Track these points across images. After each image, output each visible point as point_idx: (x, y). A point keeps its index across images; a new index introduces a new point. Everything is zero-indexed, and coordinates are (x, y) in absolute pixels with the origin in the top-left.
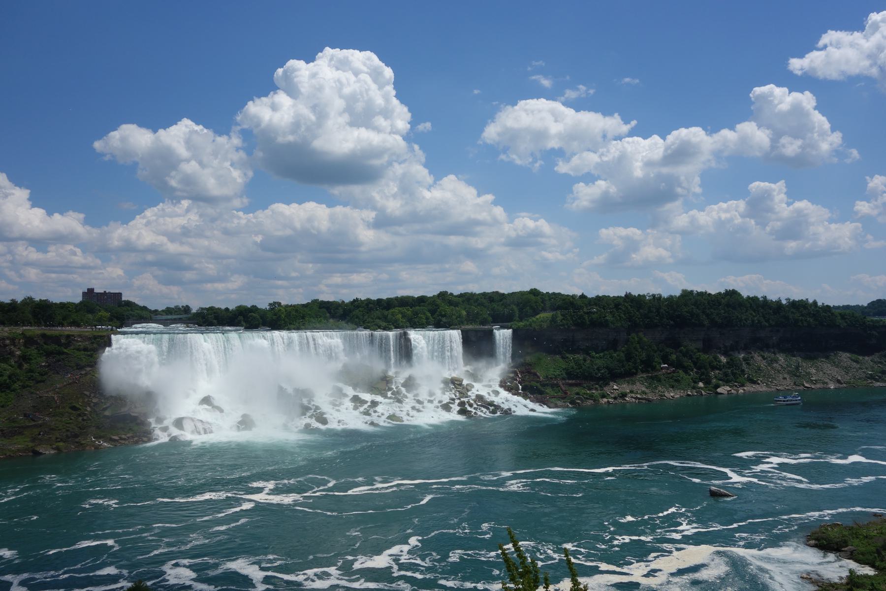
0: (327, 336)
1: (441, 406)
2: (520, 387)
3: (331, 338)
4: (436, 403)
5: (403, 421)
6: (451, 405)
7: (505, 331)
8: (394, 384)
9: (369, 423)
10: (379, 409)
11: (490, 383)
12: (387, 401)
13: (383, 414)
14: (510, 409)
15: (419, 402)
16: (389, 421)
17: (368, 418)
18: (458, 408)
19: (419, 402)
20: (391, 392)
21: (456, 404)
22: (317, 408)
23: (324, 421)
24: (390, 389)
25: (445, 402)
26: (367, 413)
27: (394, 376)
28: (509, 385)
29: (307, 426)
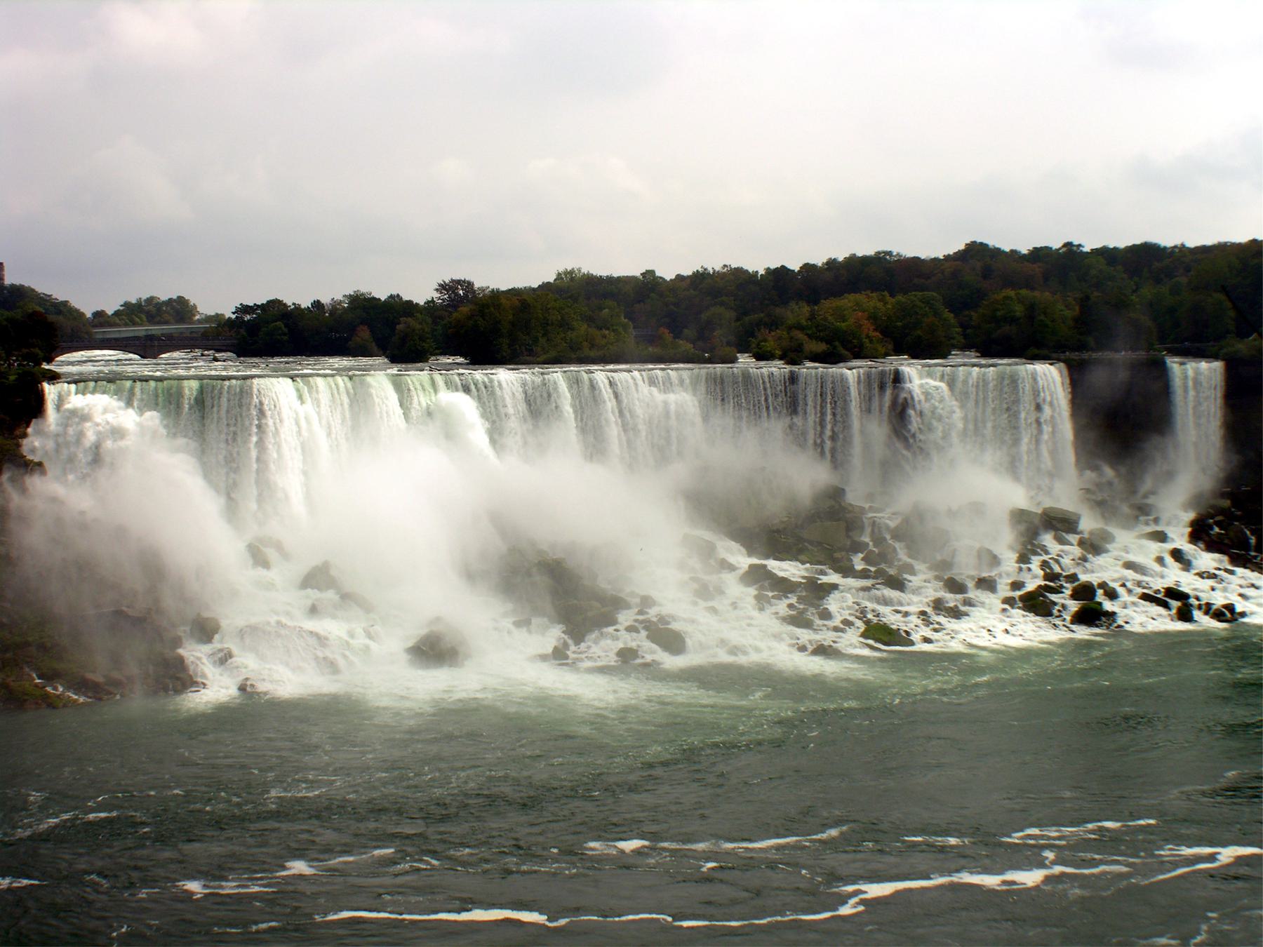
0: (652, 382)
1: (1022, 598)
2: (1253, 540)
3: (667, 386)
4: (1004, 590)
5: (912, 643)
6: (1053, 597)
7: (1204, 365)
8: (868, 530)
9: (810, 648)
10: (833, 604)
11: (1159, 528)
12: (851, 582)
13: (847, 623)
14: (1230, 608)
15: (955, 586)
16: (871, 642)
17: (805, 635)
18: (1074, 606)
19: (955, 586)
20: (861, 555)
21: (1068, 592)
22: (647, 602)
23: (672, 641)
24: (857, 547)
25: (1031, 586)
26: (799, 620)
27: (867, 506)
28: (1218, 533)
29: (627, 655)
